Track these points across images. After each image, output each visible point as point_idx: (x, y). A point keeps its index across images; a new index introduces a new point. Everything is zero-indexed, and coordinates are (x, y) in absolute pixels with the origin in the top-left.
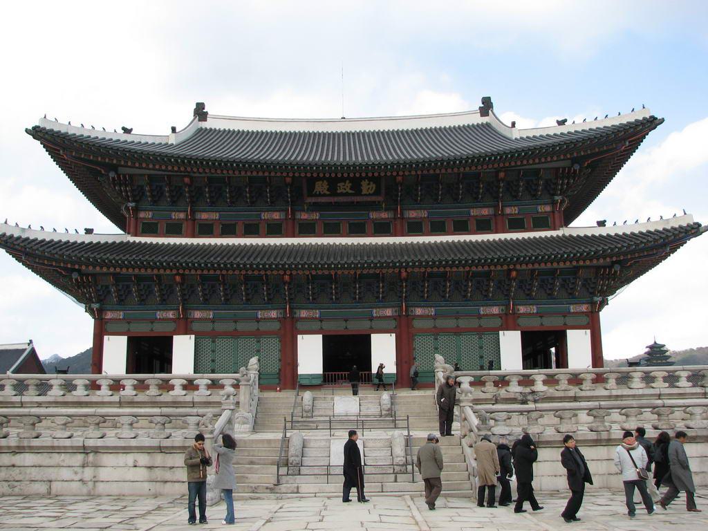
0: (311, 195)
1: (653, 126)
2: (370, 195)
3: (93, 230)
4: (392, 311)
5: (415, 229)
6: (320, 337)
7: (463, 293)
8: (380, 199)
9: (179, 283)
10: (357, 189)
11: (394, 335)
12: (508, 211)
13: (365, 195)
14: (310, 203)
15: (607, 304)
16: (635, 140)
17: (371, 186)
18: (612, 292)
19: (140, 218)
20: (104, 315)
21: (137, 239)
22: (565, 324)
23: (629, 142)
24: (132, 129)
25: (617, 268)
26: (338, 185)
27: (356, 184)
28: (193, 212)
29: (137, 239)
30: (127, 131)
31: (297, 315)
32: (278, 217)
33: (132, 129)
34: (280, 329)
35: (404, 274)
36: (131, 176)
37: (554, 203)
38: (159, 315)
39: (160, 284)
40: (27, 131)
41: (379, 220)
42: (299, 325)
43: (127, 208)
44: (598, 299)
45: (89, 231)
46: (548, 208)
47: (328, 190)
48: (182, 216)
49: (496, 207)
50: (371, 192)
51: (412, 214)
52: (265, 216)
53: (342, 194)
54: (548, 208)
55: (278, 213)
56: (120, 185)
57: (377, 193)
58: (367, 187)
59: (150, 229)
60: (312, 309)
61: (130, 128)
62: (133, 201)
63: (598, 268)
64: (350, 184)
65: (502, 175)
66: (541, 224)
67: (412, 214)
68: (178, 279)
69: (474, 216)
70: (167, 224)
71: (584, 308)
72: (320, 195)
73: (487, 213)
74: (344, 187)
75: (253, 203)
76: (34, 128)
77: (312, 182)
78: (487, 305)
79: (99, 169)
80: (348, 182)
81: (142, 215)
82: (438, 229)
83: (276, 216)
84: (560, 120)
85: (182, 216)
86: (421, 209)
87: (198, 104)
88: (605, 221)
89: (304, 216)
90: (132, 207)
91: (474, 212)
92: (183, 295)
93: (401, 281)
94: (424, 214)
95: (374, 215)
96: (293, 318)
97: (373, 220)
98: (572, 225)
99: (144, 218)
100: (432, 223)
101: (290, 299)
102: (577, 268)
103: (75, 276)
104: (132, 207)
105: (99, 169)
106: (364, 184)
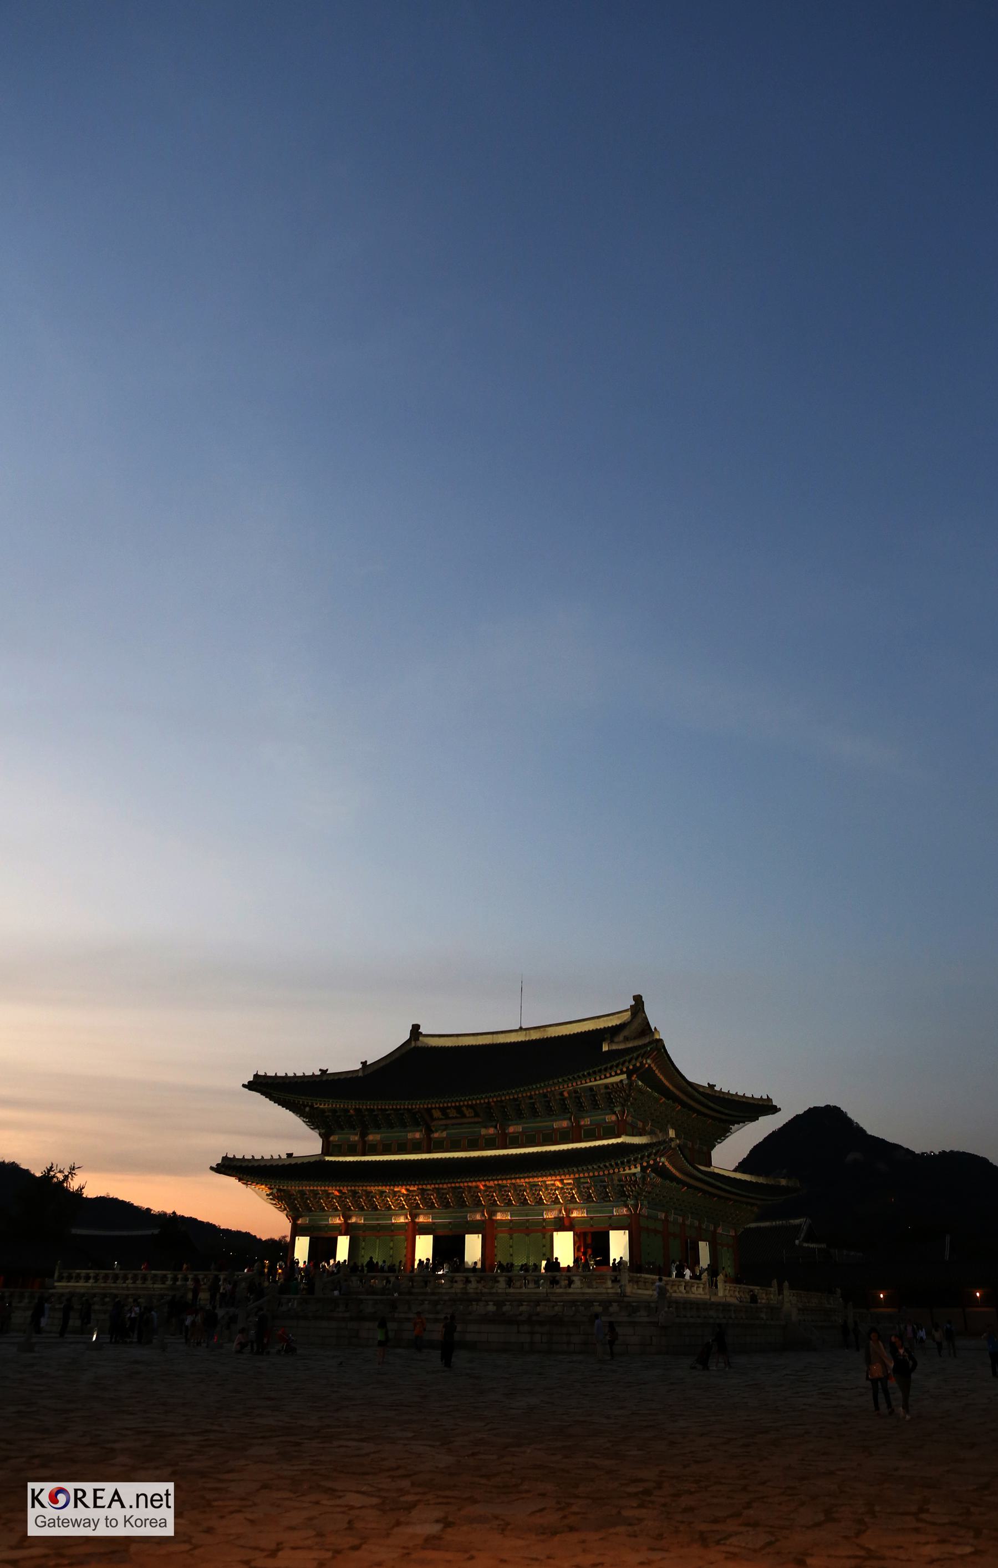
6: (431, 1237)
30: (324, 1072)
40: (244, 1086)
45: (290, 1155)
46: (614, 1118)
52: (410, 1136)
85: (356, 1138)
86: (517, 1124)
97: (484, 1136)
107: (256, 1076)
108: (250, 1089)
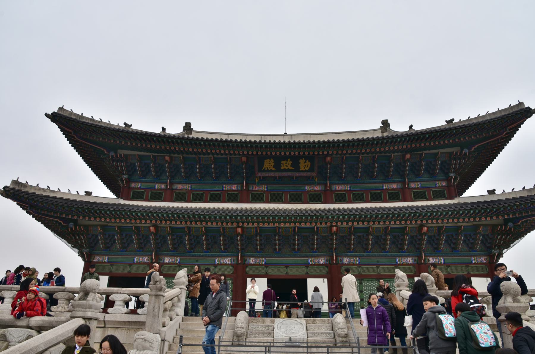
0: (261, 170)
1: (529, 115)
2: (306, 171)
3: (91, 193)
4: (325, 260)
5: (341, 199)
7: (382, 246)
8: (314, 174)
9: (153, 232)
10: (296, 167)
11: (326, 280)
12: (412, 185)
13: (302, 171)
14: (260, 177)
15: (502, 257)
16: (502, 138)
17: (306, 164)
18: (508, 246)
19: (132, 188)
20: (92, 258)
21: (127, 202)
22: (469, 273)
23: (509, 130)
24: (131, 125)
25: (510, 225)
26: (282, 162)
27: (295, 161)
28: (171, 184)
29: (127, 202)
31: (247, 262)
32: (235, 189)
33: (131, 125)
34: (233, 273)
35: (334, 229)
36: (126, 156)
37: (448, 180)
38: (136, 259)
39: (138, 233)
40: (47, 115)
41: (312, 192)
42: (248, 270)
43: (122, 180)
44: (496, 252)
45: (88, 194)
46: (444, 184)
47: (274, 167)
48: (163, 186)
49: (404, 183)
50: (307, 169)
51: (338, 188)
52: (226, 187)
53: (284, 170)
54: (444, 184)
55: (236, 186)
56: (117, 161)
57: (311, 169)
58: (304, 165)
59: (138, 196)
60: (260, 257)
61: (130, 124)
62: (126, 175)
63: (494, 226)
64: (291, 162)
65: (408, 156)
66: (439, 195)
67: (338, 188)
68: (152, 229)
69: (386, 189)
70: (152, 193)
71: (484, 260)
72: (268, 171)
73: (396, 187)
74: (287, 165)
75: (217, 178)
76: (54, 113)
77: (262, 159)
78: (402, 256)
79: (102, 149)
80: (289, 160)
81: (133, 185)
82: (359, 199)
83: (234, 187)
84: (448, 120)
85: (163, 186)
86: (345, 184)
87: (186, 123)
88: (495, 190)
89: (255, 188)
90: (125, 178)
91: (385, 186)
92: (156, 244)
93: (332, 235)
94: (348, 187)
95: (308, 188)
96: (244, 264)
98: (463, 196)
99: (136, 188)
100: (354, 194)
101: (242, 249)
102: (477, 227)
103: (71, 225)
104: (125, 178)
105: (102, 149)
106: (302, 161)
107: (61, 109)
108: (53, 121)
